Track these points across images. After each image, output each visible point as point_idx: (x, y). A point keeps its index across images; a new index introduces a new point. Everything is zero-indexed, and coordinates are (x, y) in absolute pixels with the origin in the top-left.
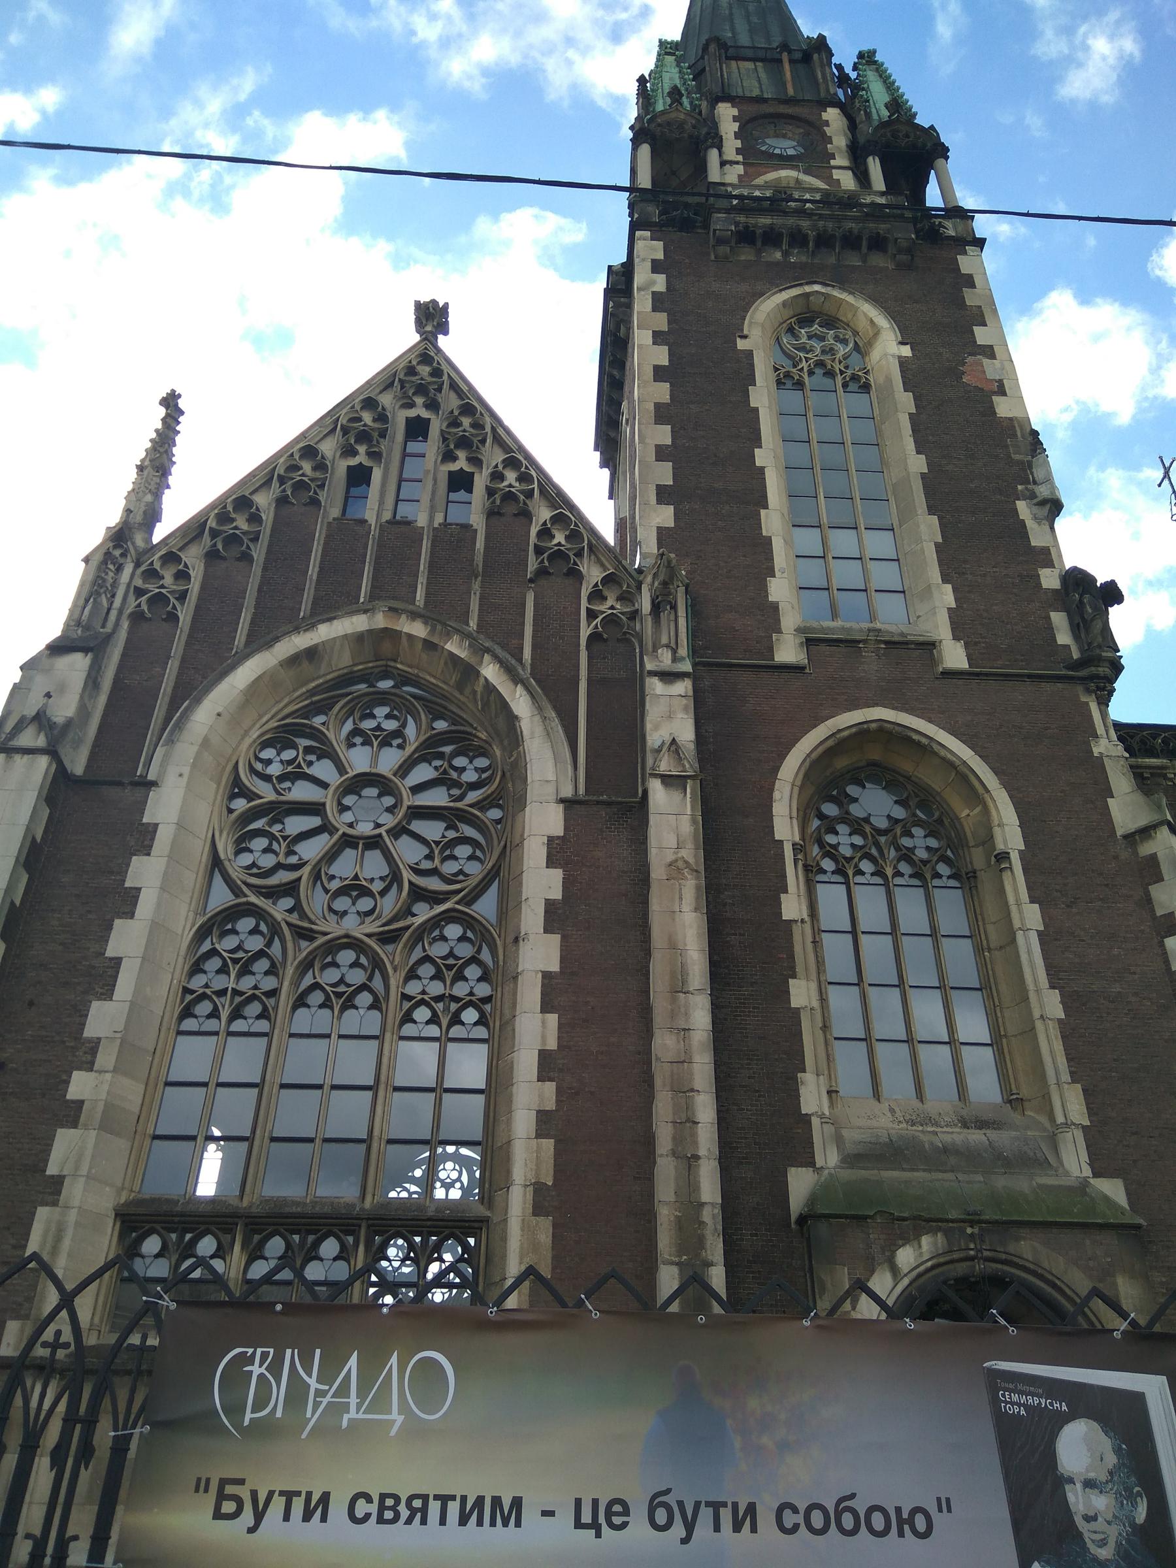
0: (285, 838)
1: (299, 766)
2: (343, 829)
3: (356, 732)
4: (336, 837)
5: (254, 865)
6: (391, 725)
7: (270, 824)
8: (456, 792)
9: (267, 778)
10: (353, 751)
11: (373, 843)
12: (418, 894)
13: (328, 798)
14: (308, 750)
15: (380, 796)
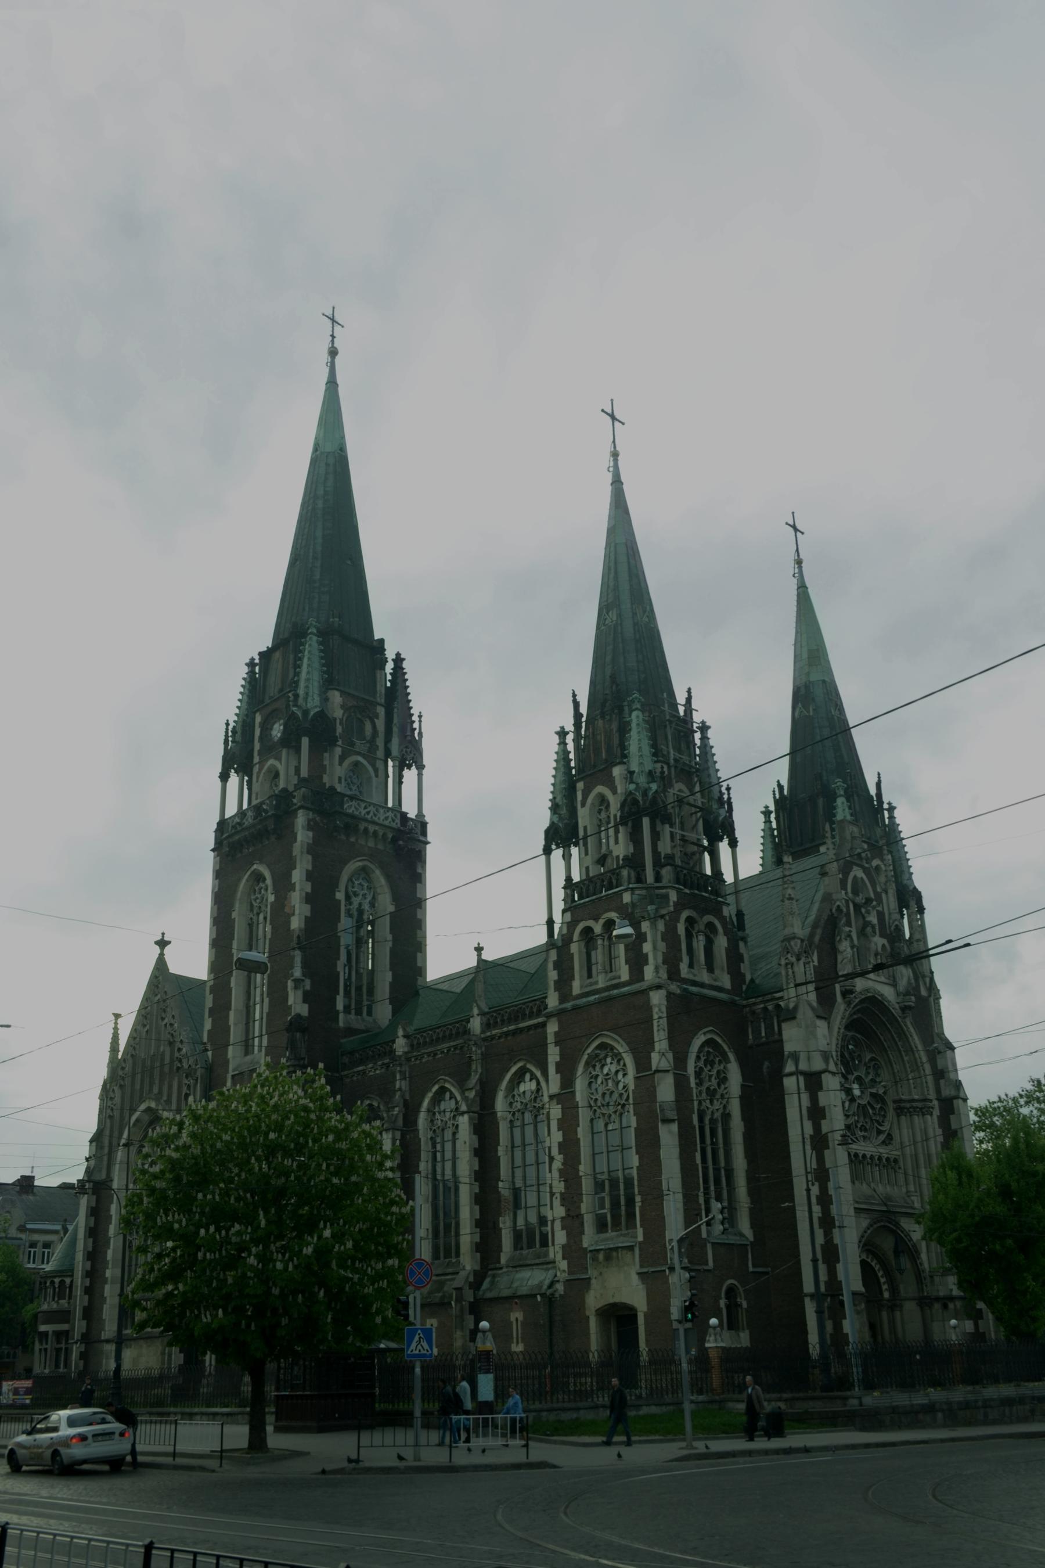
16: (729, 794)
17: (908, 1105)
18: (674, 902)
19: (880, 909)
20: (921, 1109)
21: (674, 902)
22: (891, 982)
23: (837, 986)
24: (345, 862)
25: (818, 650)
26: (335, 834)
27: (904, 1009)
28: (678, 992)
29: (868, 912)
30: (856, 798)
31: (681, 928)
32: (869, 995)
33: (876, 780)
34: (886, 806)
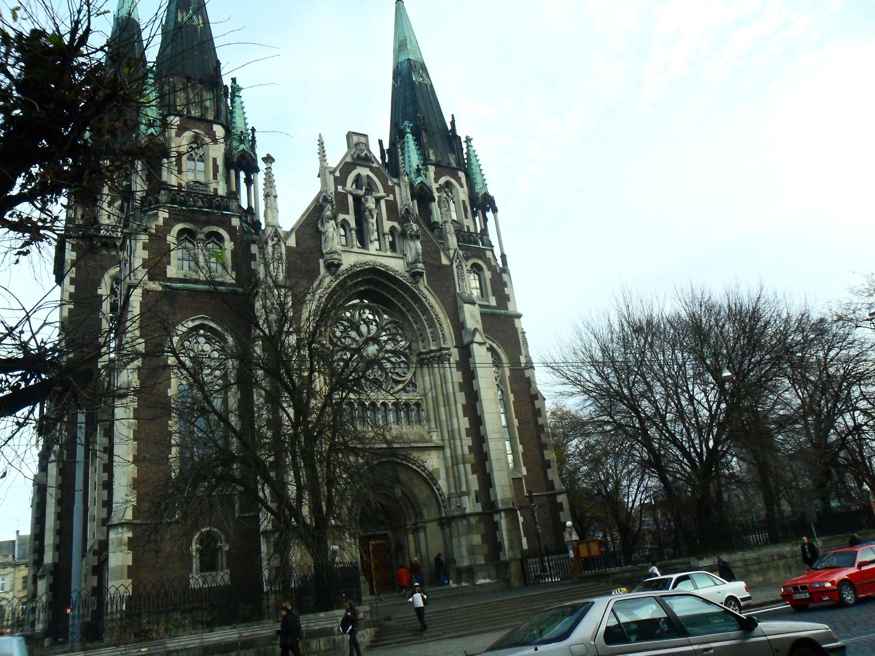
16: (253, 134)
17: (429, 356)
18: (164, 218)
19: (391, 197)
20: (439, 357)
21: (164, 218)
22: (401, 256)
23: (321, 261)
24: (105, 269)
25: (405, 40)
26: (95, 251)
27: (416, 276)
28: (160, 288)
29: (366, 200)
30: (424, 133)
32: (367, 267)
33: (451, 120)
34: (463, 139)
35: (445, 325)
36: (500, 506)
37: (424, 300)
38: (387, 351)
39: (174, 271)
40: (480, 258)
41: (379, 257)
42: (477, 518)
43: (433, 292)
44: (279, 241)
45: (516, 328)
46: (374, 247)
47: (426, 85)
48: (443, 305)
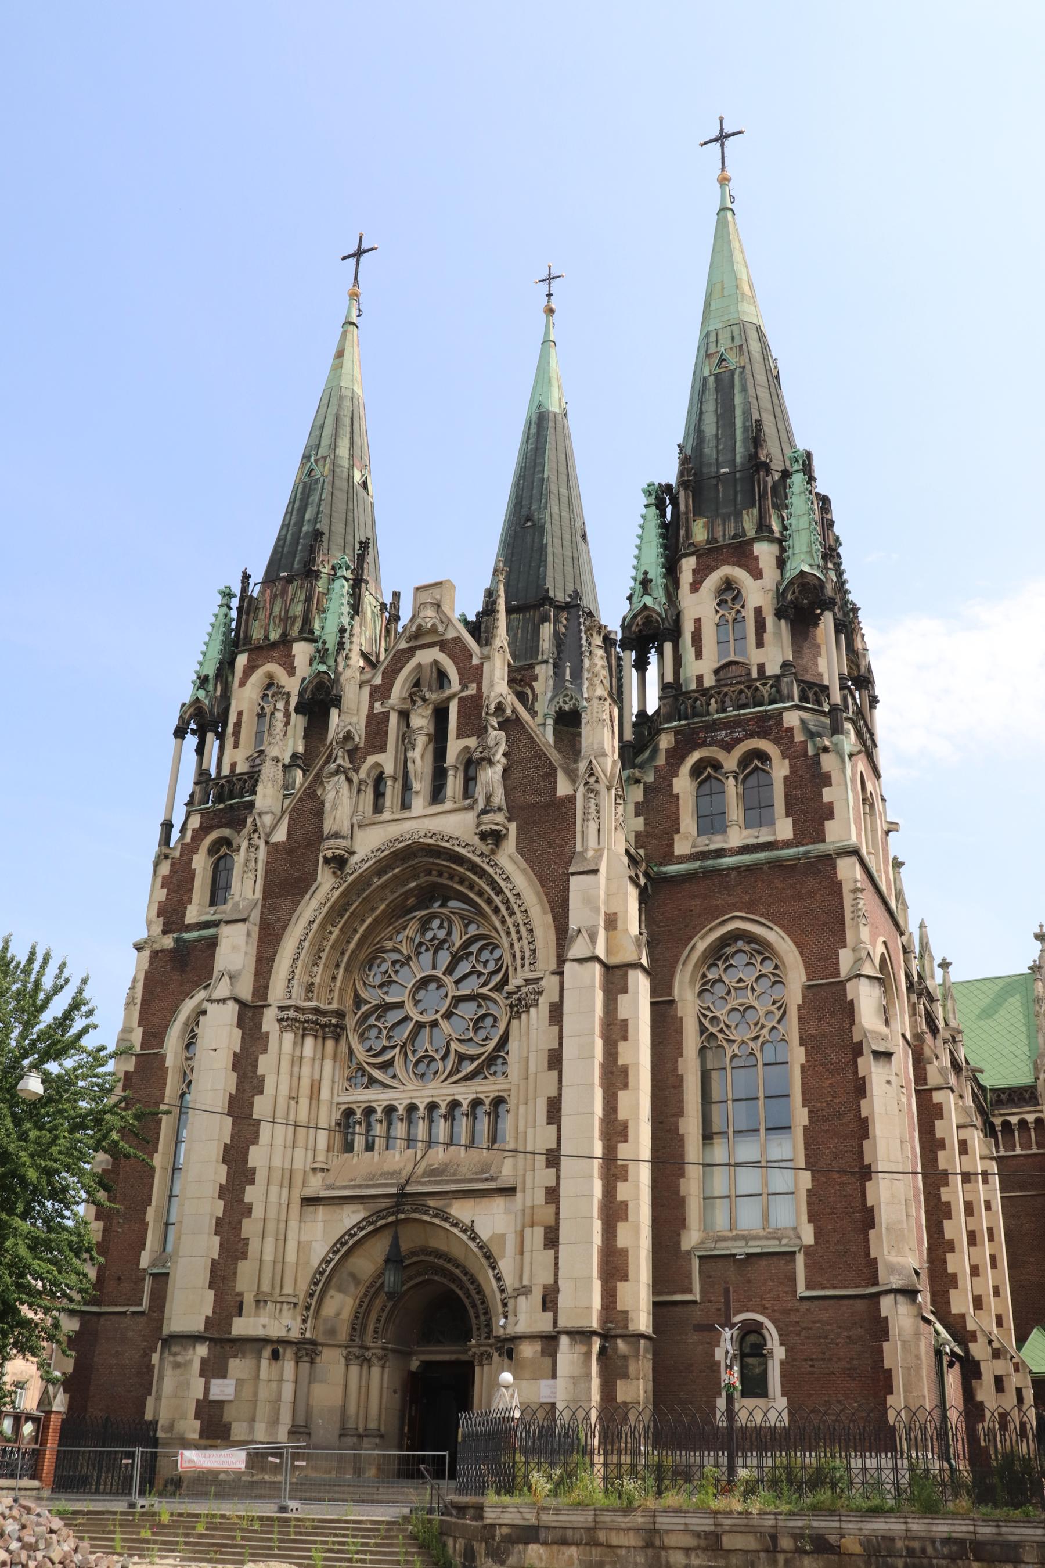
0: (385, 1028)
1: (390, 976)
2: (416, 1018)
3: (421, 944)
4: (412, 1024)
5: (370, 1049)
6: (442, 934)
7: (378, 1019)
8: (483, 979)
9: (374, 987)
10: (421, 957)
11: (434, 1024)
12: (462, 1058)
13: (404, 996)
14: (394, 963)
15: (437, 988)
18: (194, 830)
19: (472, 690)
21: (194, 830)
31: (201, 862)
35: (538, 932)
36: (562, 1323)
37: (502, 884)
38: (458, 1000)
39: (195, 913)
40: (764, 734)
41: (426, 821)
42: (538, 1346)
43: (524, 865)
44: (259, 838)
45: (840, 884)
46: (419, 805)
47: (733, 372)
48: (543, 886)
